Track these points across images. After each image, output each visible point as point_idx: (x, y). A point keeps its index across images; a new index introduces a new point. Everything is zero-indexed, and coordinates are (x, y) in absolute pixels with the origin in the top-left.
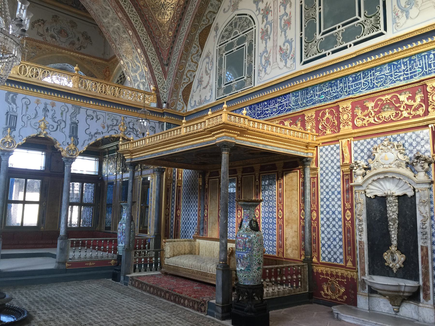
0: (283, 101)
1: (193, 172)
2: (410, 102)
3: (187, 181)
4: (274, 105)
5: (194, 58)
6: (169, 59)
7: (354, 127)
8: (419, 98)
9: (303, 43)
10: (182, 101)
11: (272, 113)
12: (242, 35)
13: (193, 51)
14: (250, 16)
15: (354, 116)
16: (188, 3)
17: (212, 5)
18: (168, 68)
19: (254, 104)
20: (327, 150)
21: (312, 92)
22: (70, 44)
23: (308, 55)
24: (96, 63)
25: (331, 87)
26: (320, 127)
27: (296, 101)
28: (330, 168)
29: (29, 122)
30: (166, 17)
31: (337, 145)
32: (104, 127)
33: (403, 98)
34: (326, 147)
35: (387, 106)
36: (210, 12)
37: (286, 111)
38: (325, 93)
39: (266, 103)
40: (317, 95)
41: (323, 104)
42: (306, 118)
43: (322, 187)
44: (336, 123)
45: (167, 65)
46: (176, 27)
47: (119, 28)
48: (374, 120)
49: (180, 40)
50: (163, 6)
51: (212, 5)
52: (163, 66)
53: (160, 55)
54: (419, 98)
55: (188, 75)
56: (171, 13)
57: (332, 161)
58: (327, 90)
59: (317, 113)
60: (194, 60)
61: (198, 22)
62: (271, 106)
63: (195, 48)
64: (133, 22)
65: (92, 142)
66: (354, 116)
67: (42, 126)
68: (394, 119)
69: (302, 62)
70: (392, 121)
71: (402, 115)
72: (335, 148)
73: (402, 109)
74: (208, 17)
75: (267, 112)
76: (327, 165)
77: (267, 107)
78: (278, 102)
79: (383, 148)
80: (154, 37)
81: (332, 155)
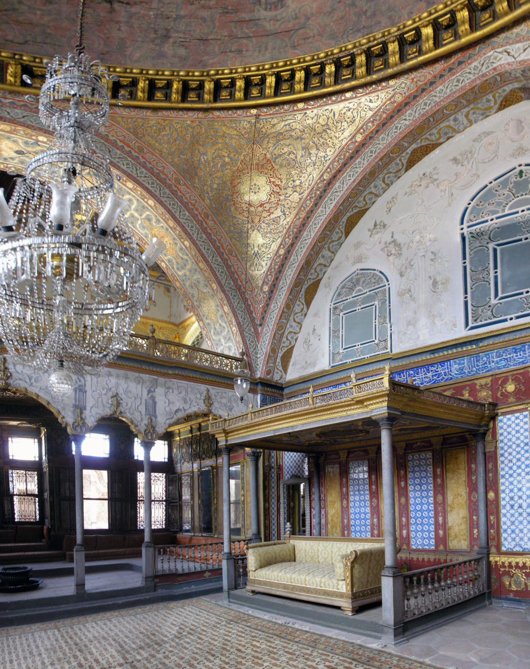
5: (297, 317)
6: (263, 318)
13: (297, 309)
16: (290, 253)
17: (323, 257)
18: (263, 329)
30: (260, 268)
36: (320, 264)
45: (261, 325)
46: (273, 281)
47: (198, 282)
49: (280, 295)
50: (256, 256)
51: (323, 257)
52: (255, 326)
53: (252, 314)
55: (289, 338)
60: (297, 320)
61: (305, 276)
63: (299, 305)
64: (218, 274)
74: (318, 270)
80: (244, 293)
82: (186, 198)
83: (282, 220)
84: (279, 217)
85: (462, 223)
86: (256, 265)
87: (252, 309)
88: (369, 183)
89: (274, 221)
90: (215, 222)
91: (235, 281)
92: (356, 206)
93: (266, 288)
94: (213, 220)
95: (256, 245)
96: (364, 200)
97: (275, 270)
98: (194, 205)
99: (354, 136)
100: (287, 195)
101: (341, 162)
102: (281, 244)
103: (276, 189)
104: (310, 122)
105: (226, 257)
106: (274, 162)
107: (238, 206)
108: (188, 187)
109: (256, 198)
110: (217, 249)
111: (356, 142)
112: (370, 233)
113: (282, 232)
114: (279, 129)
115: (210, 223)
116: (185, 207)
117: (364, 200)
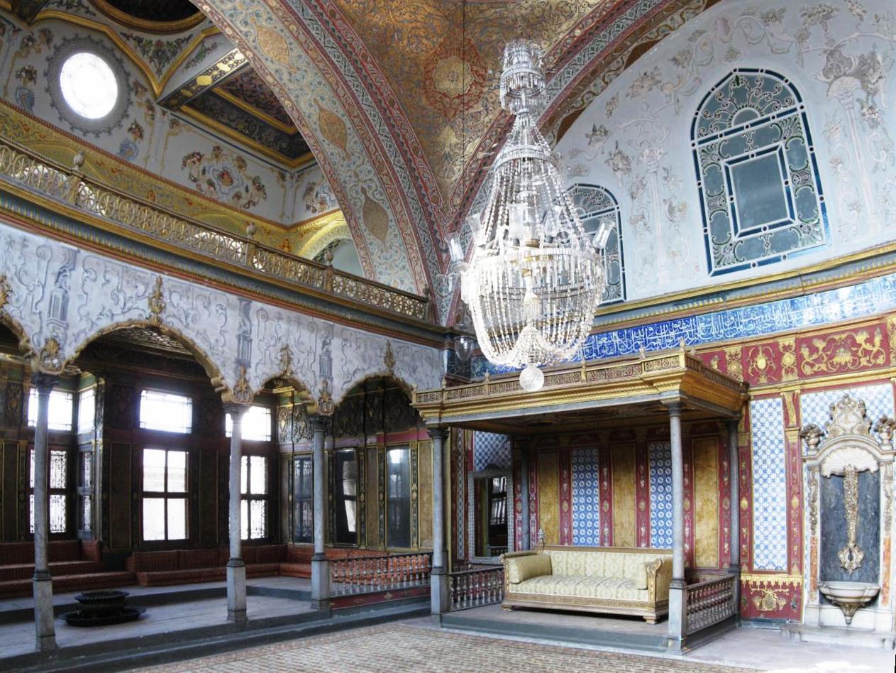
0: (683, 328)
1: (497, 439)
2: (868, 347)
3: (486, 454)
4: (668, 333)
7: (802, 375)
8: (878, 340)
9: (711, 245)
11: (664, 346)
12: (592, 217)
14: (606, 190)
15: (800, 358)
19: (627, 329)
20: (762, 406)
21: (732, 318)
22: (233, 198)
23: (721, 263)
24: (269, 233)
25: (763, 313)
26: (750, 371)
27: (708, 330)
28: (768, 433)
29: (268, 352)
31: (779, 400)
32: (365, 361)
33: (861, 338)
34: (761, 402)
35: (842, 350)
37: (692, 343)
38: (755, 321)
39: (651, 329)
40: (741, 323)
41: (753, 337)
42: (727, 358)
43: (756, 462)
44: (774, 368)
48: (827, 367)
50: (446, 158)
54: (878, 340)
56: (459, 170)
57: (771, 424)
58: (757, 318)
59: (745, 351)
62: (663, 334)
65: (349, 386)
66: (800, 358)
67: (286, 357)
68: (852, 368)
69: (712, 272)
70: (848, 371)
71: (860, 363)
72: (774, 405)
73: (860, 354)
75: (655, 344)
76: (763, 429)
77: (655, 335)
78: (675, 329)
79: (843, 406)
80: (427, 205)
81: (771, 414)
82: (371, 79)
83: (482, 117)
84: (480, 112)
85: (692, 138)
86: (446, 170)
87: (436, 228)
88: (590, 82)
89: (472, 117)
90: (401, 112)
91: (419, 189)
92: (573, 107)
93: (458, 201)
94: (399, 109)
95: (448, 145)
96: (582, 100)
97: (470, 179)
98: (379, 89)
99: (573, 31)
100: (492, 88)
101: (557, 56)
102: (480, 146)
103: (480, 80)
104: (523, 12)
105: (411, 157)
106: (480, 50)
107: (430, 95)
108: (375, 66)
109: (452, 87)
110: (400, 145)
111: (575, 36)
112: (588, 140)
113: (482, 130)
114: (488, 15)
115: (396, 113)
116: (368, 89)
117: (582, 100)
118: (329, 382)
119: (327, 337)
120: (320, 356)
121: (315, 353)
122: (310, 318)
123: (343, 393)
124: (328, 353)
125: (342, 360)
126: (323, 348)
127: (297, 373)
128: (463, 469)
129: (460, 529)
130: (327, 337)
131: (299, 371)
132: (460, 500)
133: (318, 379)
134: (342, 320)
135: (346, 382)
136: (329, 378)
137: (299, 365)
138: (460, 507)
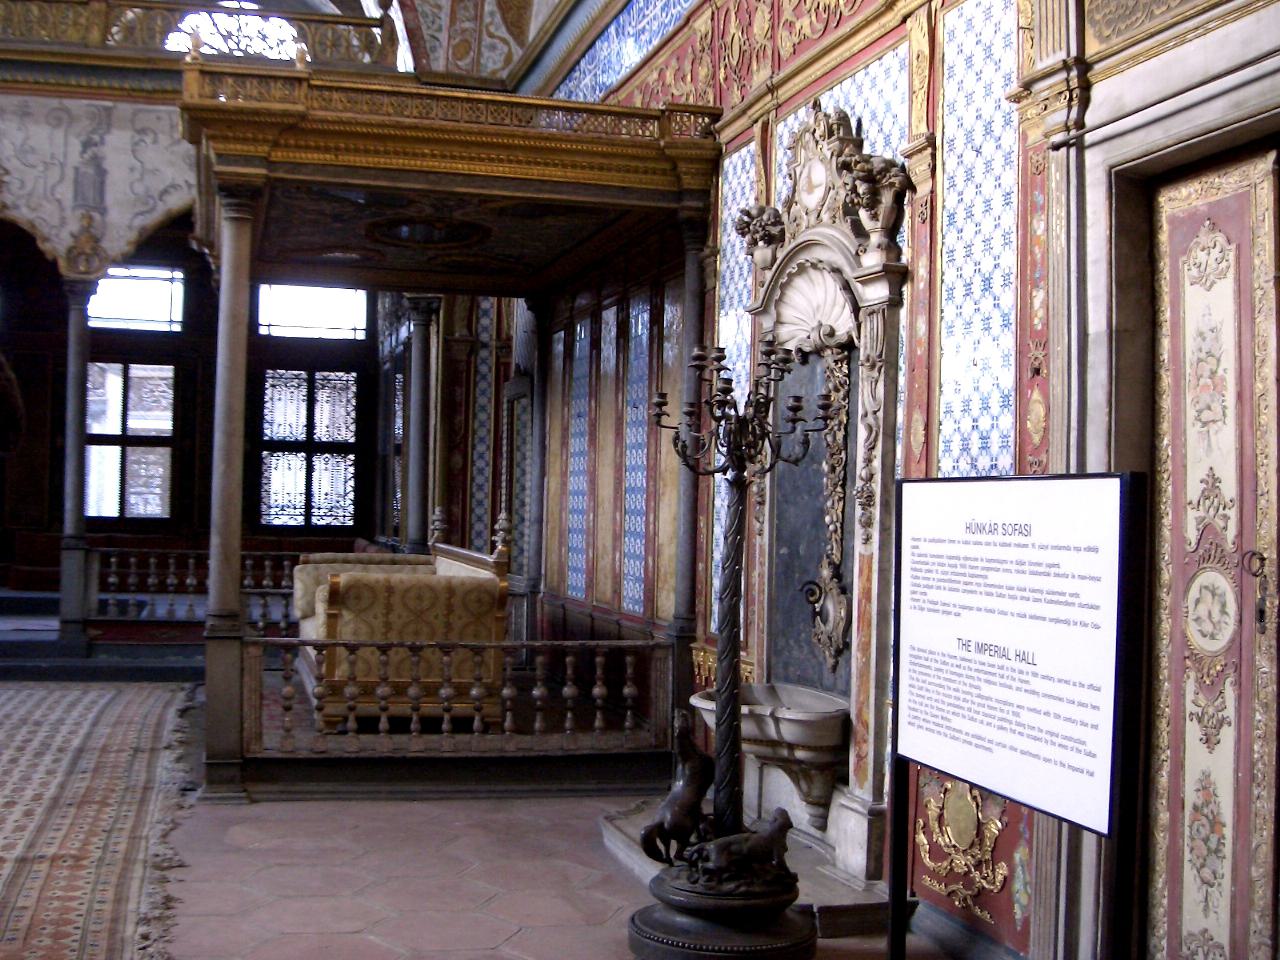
10: (503, 32)
118: (97, 216)
119: (93, 132)
120: (76, 169)
121: (62, 165)
122: (54, 102)
123: (133, 236)
124: (97, 163)
125: (132, 170)
126: (84, 151)
127: (17, 207)
128: (491, 377)
129: (479, 511)
130: (93, 132)
131: (22, 202)
132: (481, 448)
133: (68, 213)
134: (131, 95)
135: (142, 213)
136: (95, 209)
137: (21, 192)
138: (480, 464)
